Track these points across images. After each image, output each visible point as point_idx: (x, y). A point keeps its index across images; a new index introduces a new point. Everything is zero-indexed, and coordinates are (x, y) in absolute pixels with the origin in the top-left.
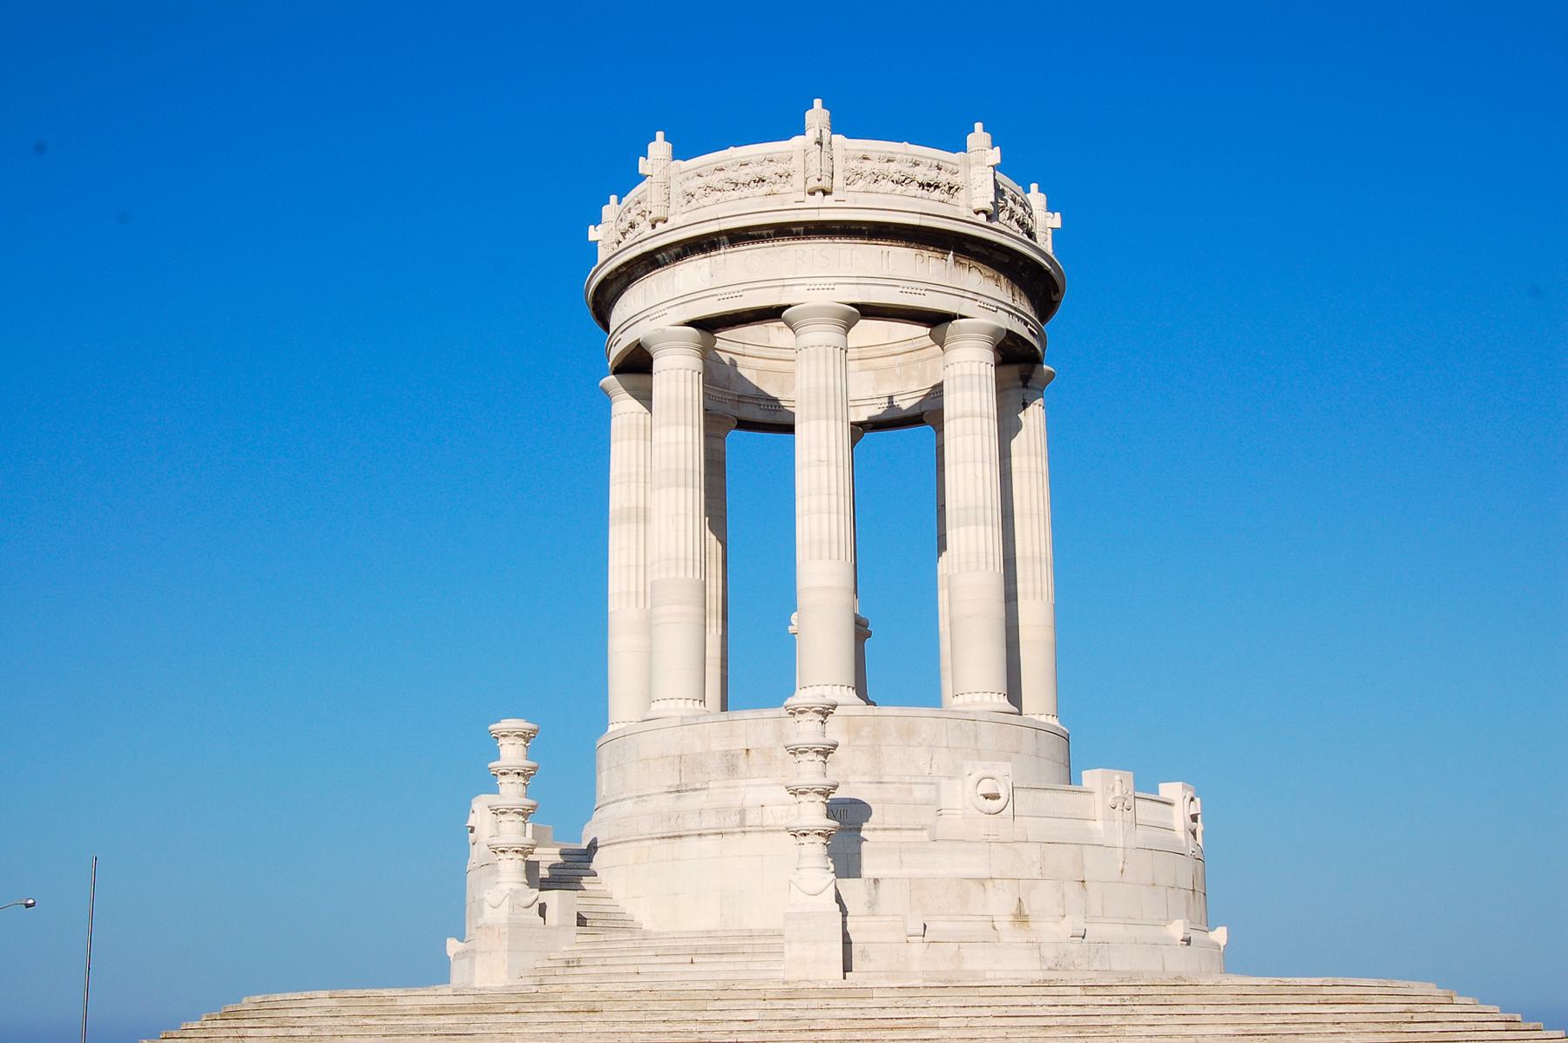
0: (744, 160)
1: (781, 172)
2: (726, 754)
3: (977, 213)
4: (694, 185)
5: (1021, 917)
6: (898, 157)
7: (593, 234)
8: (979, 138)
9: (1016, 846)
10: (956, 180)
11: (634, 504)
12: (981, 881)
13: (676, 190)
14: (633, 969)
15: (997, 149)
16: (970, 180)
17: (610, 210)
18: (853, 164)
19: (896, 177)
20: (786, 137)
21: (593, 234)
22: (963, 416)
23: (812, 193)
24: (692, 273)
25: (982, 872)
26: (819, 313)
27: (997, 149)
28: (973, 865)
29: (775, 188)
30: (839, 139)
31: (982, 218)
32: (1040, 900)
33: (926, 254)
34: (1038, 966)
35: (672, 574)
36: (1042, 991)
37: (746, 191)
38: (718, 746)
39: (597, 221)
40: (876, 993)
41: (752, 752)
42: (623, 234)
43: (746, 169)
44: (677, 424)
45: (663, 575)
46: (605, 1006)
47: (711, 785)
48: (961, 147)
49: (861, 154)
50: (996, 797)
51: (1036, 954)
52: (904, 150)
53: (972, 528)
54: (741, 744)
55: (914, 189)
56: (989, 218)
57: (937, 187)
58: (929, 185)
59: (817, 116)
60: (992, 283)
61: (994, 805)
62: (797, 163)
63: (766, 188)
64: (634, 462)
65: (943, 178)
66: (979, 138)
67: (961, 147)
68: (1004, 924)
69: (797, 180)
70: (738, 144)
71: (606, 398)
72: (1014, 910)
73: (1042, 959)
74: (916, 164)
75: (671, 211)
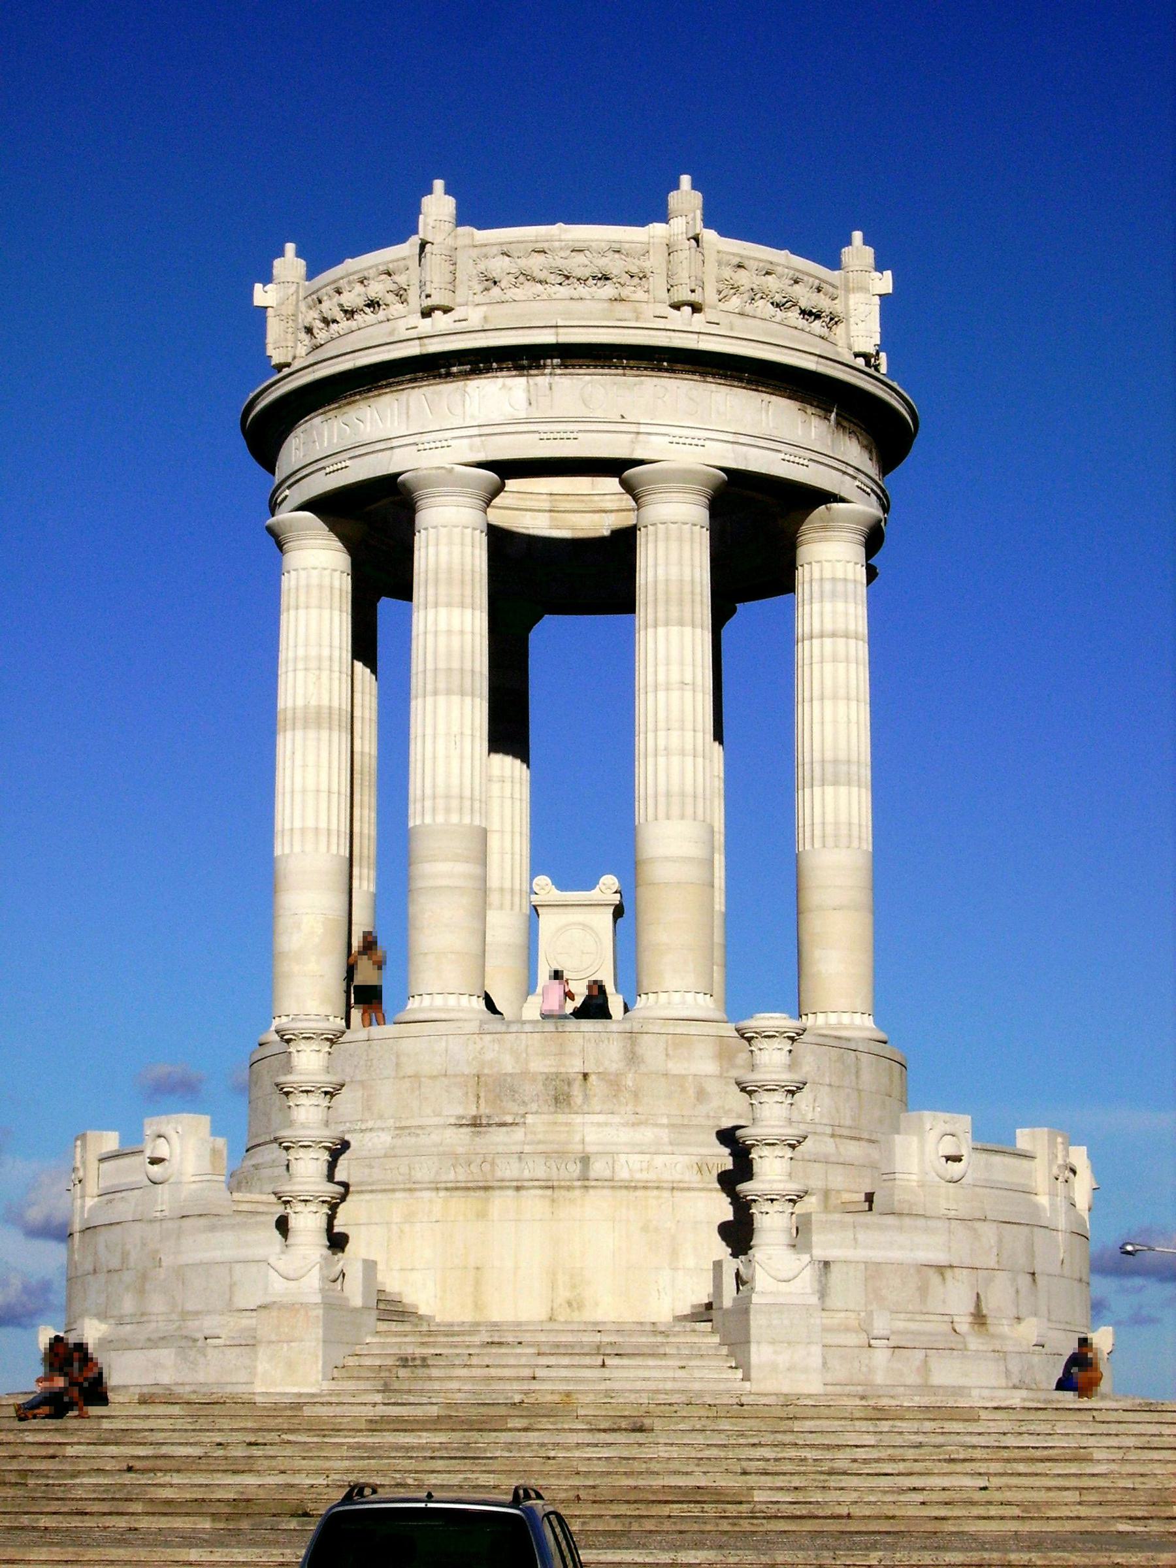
0: (578, 245)
1: (634, 270)
2: (549, 1078)
3: (857, 355)
4: (498, 266)
5: (979, 1318)
6: (779, 269)
7: (262, 295)
8: (858, 252)
9: (977, 1225)
10: (838, 307)
11: (325, 702)
12: (941, 1269)
13: (467, 269)
14: (527, 1372)
15: (888, 274)
16: (851, 309)
17: (289, 264)
18: (727, 273)
19: (778, 298)
20: (642, 222)
21: (262, 295)
22: (834, 635)
23: (677, 306)
24: (496, 398)
25: (941, 1258)
26: (683, 477)
27: (888, 274)
28: (929, 1248)
29: (625, 292)
30: (710, 236)
31: (860, 362)
32: (998, 1298)
33: (810, 410)
34: (1003, 1382)
35: (455, 819)
36: (1147, 1416)
37: (582, 290)
38: (541, 1065)
39: (267, 278)
40: (984, 1415)
41: (593, 1079)
42: (350, 313)
43: (580, 258)
44: (462, 605)
45: (440, 819)
46: (658, 1424)
47: (530, 1119)
48: (834, 263)
49: (736, 261)
50: (957, 1159)
51: (1002, 1368)
52: (781, 257)
53: (843, 790)
54: (575, 1066)
55: (793, 316)
56: (868, 364)
57: (818, 317)
58: (810, 314)
59: (686, 198)
60: (866, 456)
61: (955, 1168)
62: (655, 262)
63: (608, 290)
64: (326, 642)
65: (822, 302)
66: (858, 252)
67: (834, 263)
68: (964, 1324)
69: (658, 284)
70: (569, 221)
71: (278, 540)
72: (971, 1308)
73: (1008, 1374)
74: (796, 282)
75: (462, 293)
